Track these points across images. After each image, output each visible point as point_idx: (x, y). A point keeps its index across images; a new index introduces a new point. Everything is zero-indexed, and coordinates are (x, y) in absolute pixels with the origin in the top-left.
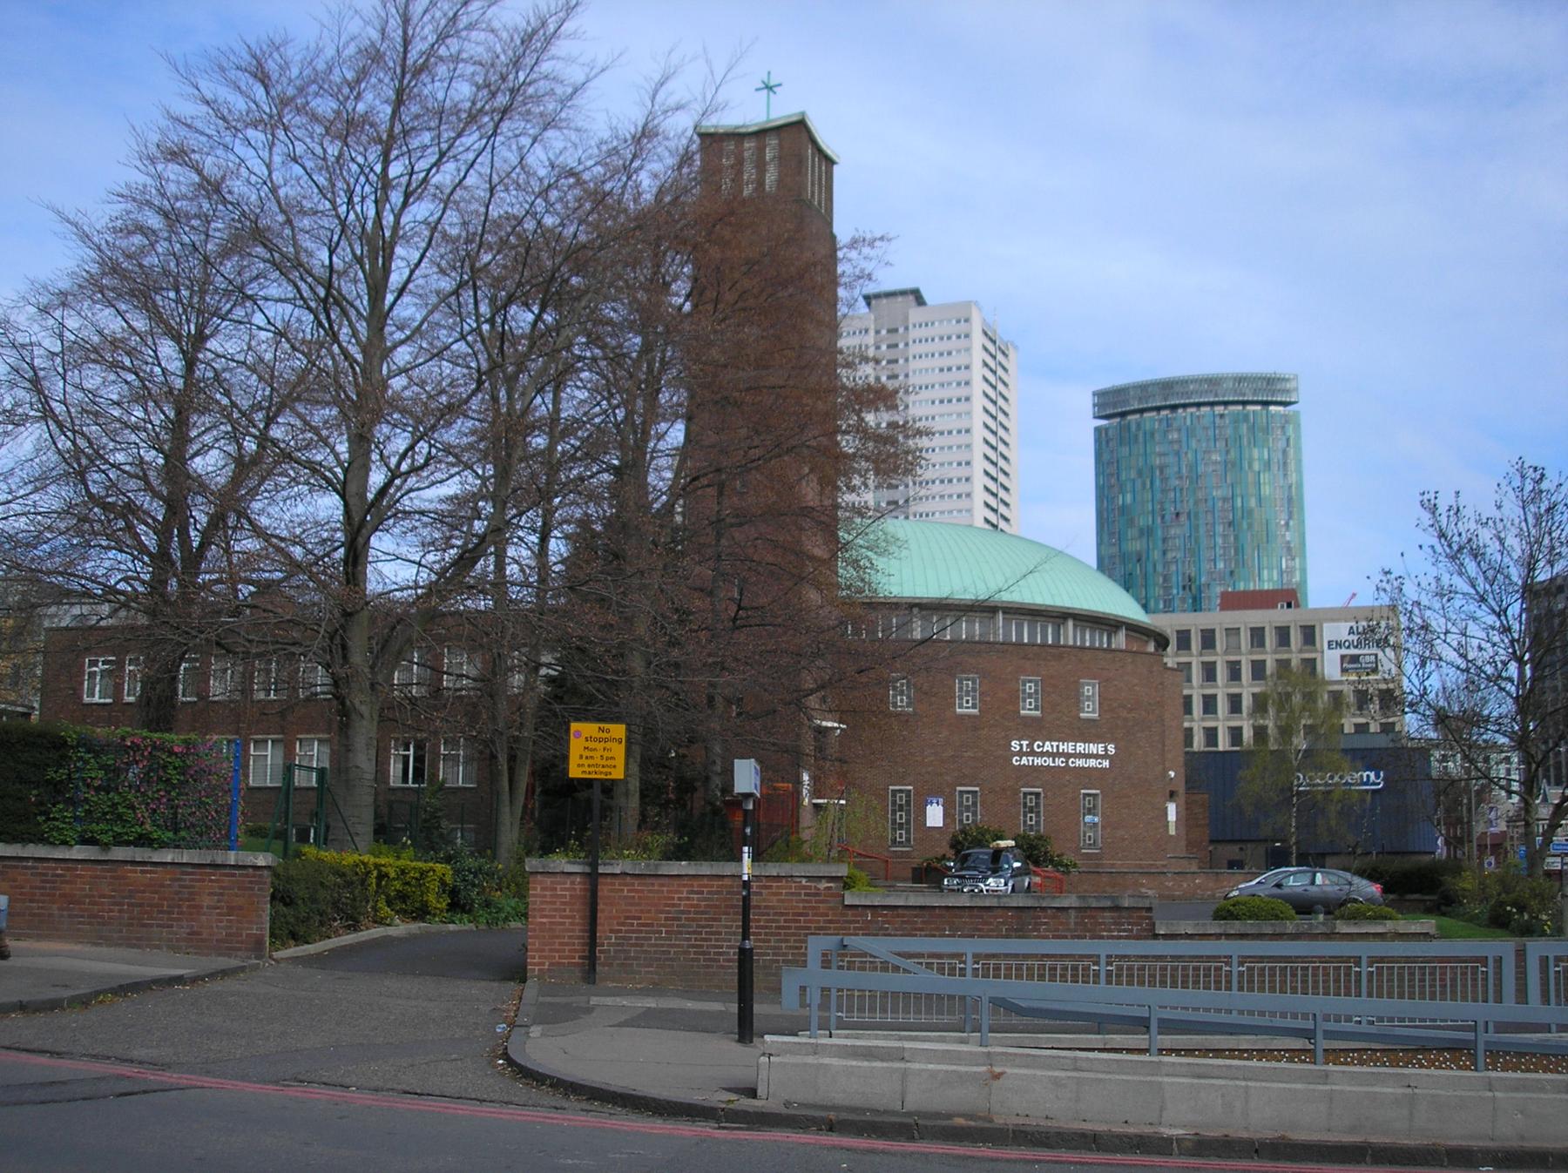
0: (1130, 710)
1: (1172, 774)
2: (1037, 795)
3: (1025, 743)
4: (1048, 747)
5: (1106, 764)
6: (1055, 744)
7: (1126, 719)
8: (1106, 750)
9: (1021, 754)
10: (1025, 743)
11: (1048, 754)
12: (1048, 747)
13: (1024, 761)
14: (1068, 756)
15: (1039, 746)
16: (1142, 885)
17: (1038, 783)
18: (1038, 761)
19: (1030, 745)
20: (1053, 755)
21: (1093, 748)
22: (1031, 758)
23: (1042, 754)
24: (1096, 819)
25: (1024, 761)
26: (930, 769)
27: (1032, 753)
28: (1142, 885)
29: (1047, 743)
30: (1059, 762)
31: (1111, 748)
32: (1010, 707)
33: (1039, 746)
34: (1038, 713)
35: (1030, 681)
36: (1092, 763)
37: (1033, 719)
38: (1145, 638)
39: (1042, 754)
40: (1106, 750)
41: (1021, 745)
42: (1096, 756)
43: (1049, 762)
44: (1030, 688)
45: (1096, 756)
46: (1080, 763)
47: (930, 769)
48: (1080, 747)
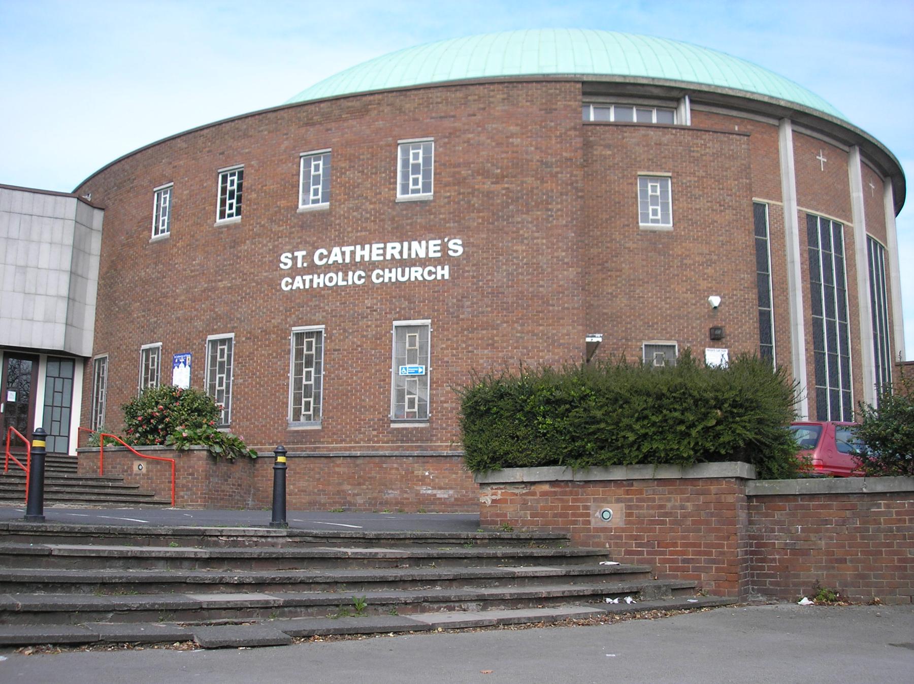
0: (499, 179)
1: (715, 300)
2: (319, 333)
3: (300, 254)
4: (336, 255)
5: (444, 272)
6: (348, 249)
7: (489, 195)
8: (444, 248)
9: (294, 272)
10: (300, 254)
11: (336, 267)
12: (336, 255)
13: (298, 283)
14: (369, 266)
15: (321, 257)
16: (423, 480)
17: (319, 316)
18: (319, 281)
19: (309, 257)
20: (343, 268)
21: (418, 249)
22: (307, 278)
23: (327, 269)
24: (421, 370)
25: (298, 283)
26: (180, 313)
27: (312, 269)
28: (423, 480)
29: (336, 250)
30: (355, 278)
31: (456, 247)
32: (282, 203)
33: (321, 257)
34: (326, 205)
35: (317, 157)
36: (416, 273)
37: (314, 214)
38: (775, 122)
39: (327, 269)
40: (444, 248)
41: (294, 259)
42: (423, 262)
43: (338, 279)
44: (318, 168)
45: (423, 262)
46: (392, 275)
47: (180, 313)
48: (393, 249)
